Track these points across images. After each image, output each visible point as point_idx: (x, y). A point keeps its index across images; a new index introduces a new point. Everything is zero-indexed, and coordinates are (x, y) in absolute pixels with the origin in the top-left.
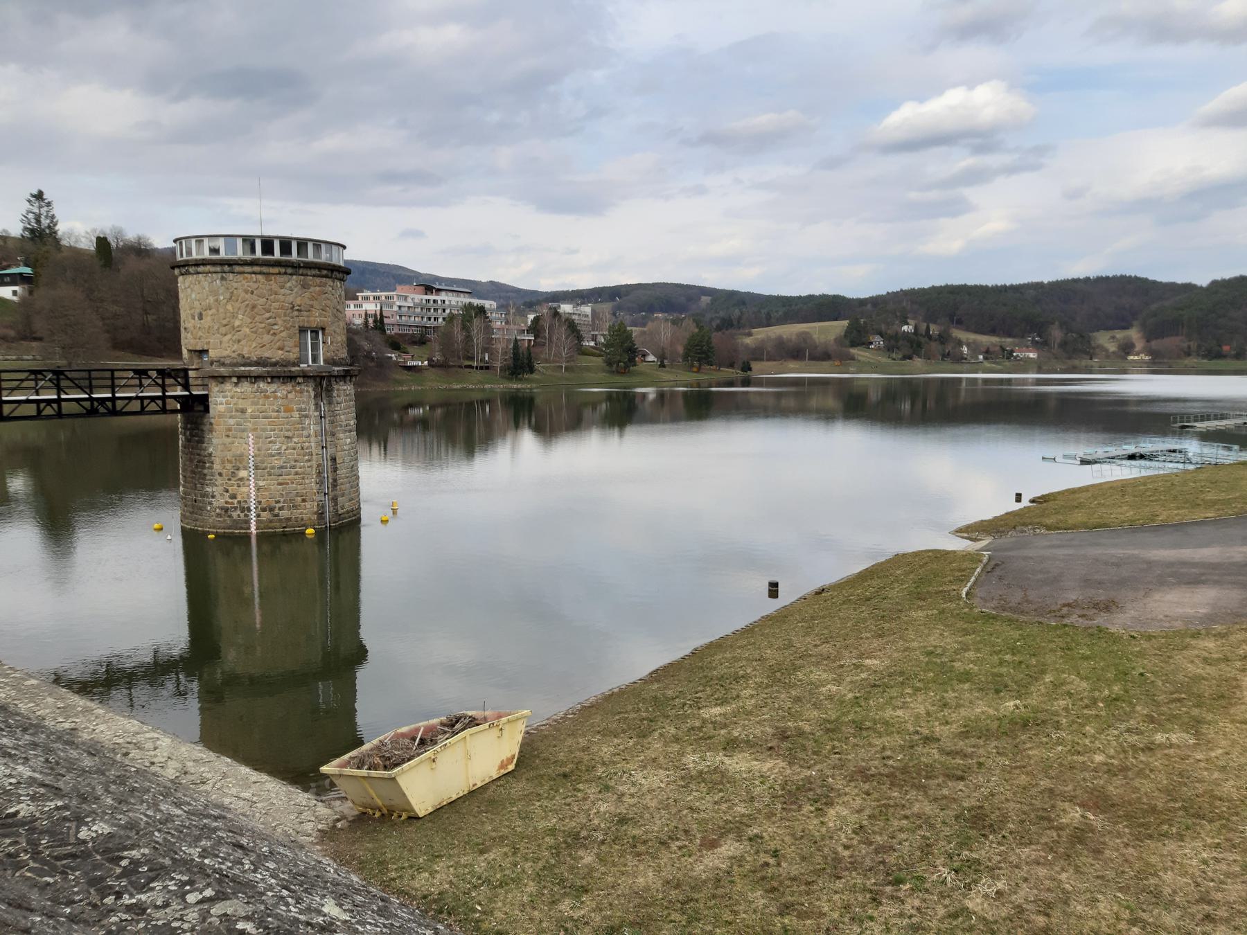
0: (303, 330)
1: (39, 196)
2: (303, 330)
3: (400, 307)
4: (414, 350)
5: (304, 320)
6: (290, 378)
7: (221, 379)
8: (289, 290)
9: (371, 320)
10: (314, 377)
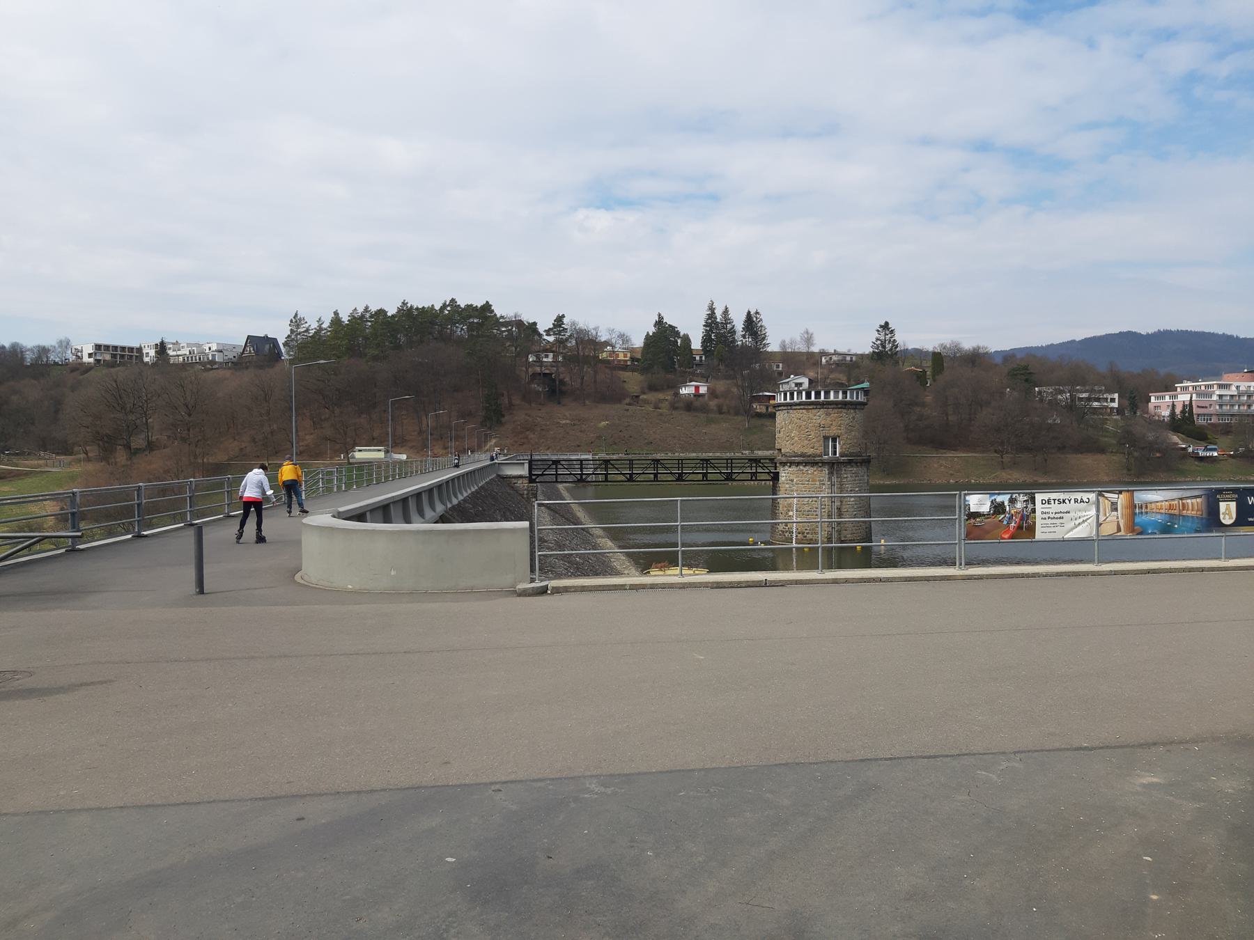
0: (826, 438)
1: (886, 326)
2: (826, 438)
3: (1221, 396)
4: (1224, 441)
5: (827, 432)
6: (814, 464)
7: (784, 464)
8: (819, 417)
9: (1178, 410)
10: (828, 463)
